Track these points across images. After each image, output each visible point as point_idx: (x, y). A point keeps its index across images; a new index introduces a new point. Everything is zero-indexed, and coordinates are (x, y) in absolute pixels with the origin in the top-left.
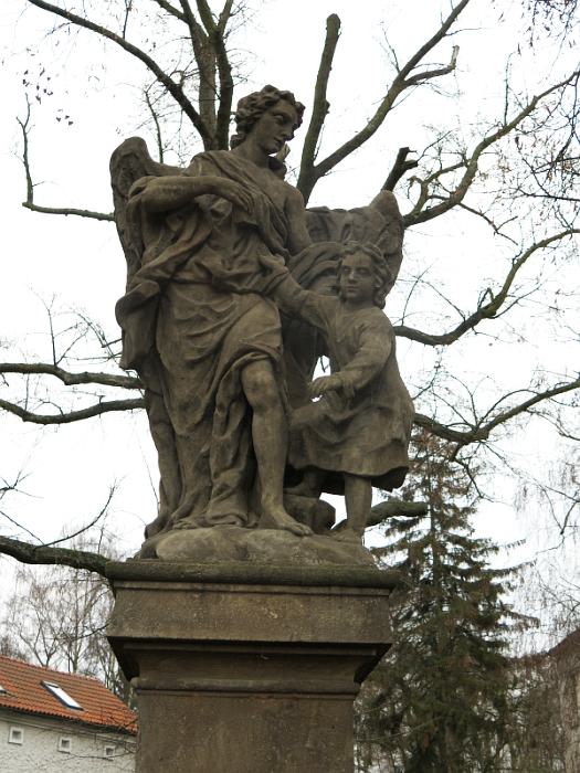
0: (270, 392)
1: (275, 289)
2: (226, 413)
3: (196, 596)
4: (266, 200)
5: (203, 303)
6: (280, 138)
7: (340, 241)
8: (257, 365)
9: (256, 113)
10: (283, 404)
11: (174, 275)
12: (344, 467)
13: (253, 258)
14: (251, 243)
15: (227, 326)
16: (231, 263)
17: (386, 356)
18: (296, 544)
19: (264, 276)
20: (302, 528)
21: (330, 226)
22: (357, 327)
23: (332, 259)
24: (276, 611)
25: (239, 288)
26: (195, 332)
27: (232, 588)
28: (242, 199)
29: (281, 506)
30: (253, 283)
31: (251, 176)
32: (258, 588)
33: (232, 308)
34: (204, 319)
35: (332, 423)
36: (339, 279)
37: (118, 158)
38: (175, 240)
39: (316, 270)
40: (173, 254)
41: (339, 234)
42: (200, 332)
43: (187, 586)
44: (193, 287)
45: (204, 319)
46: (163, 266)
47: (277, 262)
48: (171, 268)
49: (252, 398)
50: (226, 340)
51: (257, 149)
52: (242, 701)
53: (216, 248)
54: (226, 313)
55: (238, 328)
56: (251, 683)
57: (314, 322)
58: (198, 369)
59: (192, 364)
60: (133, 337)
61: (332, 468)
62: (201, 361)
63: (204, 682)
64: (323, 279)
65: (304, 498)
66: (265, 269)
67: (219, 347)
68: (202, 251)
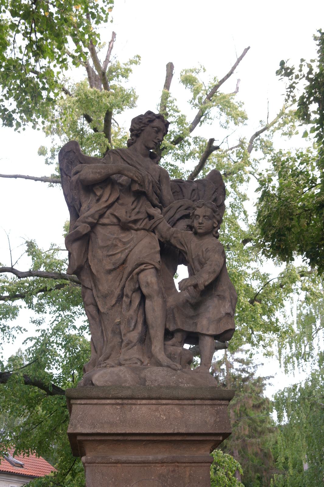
0: (156, 287)
1: (156, 227)
2: (129, 300)
3: (118, 407)
4: (150, 177)
5: (115, 236)
6: (156, 141)
7: (190, 199)
9: (142, 127)
10: (163, 294)
11: (98, 221)
12: (199, 330)
13: (143, 210)
14: (141, 202)
15: (129, 250)
16: (131, 213)
17: (221, 266)
18: (174, 375)
19: (150, 220)
20: (176, 366)
21: (184, 190)
22: (204, 250)
23: (186, 209)
24: (165, 415)
25: (136, 228)
26: (111, 253)
27: (139, 402)
28: (137, 177)
29: (163, 353)
30: (143, 224)
31: (140, 163)
32: (154, 402)
33: (132, 239)
34: (116, 245)
35: (190, 304)
36: (193, 221)
37: (64, 153)
38: (98, 200)
39: (177, 216)
40: (98, 209)
41: (189, 195)
42: (115, 253)
43: (113, 401)
44: (110, 227)
45: (116, 245)
46: (92, 216)
47: (156, 212)
48: (97, 216)
49: (145, 290)
50: (129, 257)
51: (143, 147)
52: (146, 468)
53: (122, 204)
54: (128, 242)
55: (136, 250)
56: (151, 458)
57: (179, 246)
58: (114, 274)
59: (110, 272)
60: (75, 257)
61: (191, 330)
62: (115, 269)
63: (123, 457)
64: (181, 221)
65: (174, 347)
66: (150, 217)
67: (124, 262)
68: (114, 207)
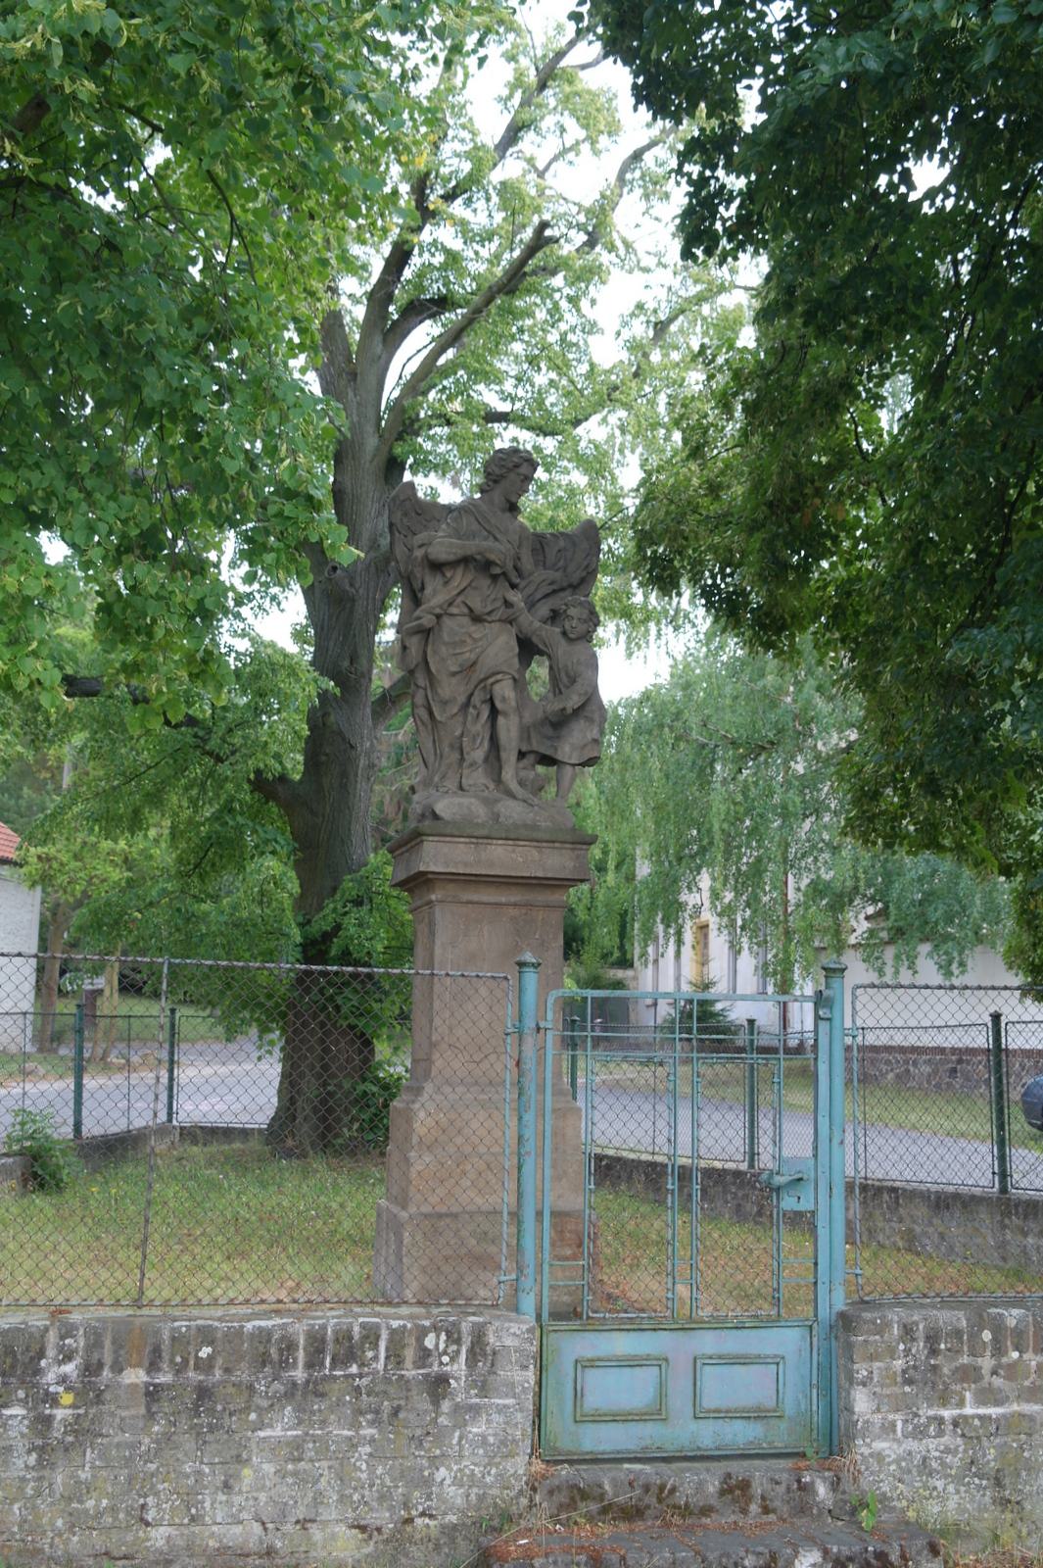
0: (513, 704)
8: (504, 683)
13: (500, 596)
33: (486, 635)
38: (446, 583)
39: (538, 595)
49: (499, 705)
53: (475, 588)
56: (504, 900)
58: (458, 677)
59: (454, 674)
63: (475, 897)
66: (508, 604)
